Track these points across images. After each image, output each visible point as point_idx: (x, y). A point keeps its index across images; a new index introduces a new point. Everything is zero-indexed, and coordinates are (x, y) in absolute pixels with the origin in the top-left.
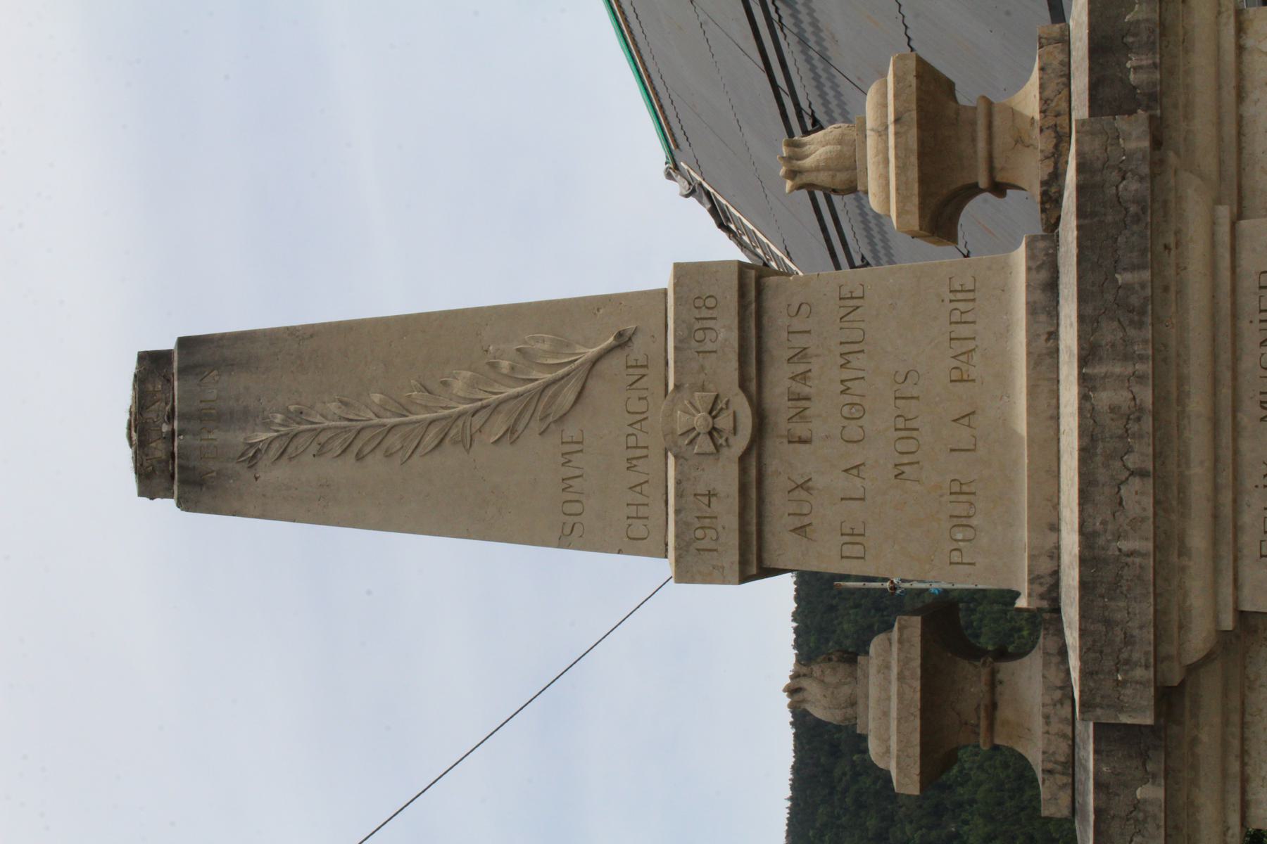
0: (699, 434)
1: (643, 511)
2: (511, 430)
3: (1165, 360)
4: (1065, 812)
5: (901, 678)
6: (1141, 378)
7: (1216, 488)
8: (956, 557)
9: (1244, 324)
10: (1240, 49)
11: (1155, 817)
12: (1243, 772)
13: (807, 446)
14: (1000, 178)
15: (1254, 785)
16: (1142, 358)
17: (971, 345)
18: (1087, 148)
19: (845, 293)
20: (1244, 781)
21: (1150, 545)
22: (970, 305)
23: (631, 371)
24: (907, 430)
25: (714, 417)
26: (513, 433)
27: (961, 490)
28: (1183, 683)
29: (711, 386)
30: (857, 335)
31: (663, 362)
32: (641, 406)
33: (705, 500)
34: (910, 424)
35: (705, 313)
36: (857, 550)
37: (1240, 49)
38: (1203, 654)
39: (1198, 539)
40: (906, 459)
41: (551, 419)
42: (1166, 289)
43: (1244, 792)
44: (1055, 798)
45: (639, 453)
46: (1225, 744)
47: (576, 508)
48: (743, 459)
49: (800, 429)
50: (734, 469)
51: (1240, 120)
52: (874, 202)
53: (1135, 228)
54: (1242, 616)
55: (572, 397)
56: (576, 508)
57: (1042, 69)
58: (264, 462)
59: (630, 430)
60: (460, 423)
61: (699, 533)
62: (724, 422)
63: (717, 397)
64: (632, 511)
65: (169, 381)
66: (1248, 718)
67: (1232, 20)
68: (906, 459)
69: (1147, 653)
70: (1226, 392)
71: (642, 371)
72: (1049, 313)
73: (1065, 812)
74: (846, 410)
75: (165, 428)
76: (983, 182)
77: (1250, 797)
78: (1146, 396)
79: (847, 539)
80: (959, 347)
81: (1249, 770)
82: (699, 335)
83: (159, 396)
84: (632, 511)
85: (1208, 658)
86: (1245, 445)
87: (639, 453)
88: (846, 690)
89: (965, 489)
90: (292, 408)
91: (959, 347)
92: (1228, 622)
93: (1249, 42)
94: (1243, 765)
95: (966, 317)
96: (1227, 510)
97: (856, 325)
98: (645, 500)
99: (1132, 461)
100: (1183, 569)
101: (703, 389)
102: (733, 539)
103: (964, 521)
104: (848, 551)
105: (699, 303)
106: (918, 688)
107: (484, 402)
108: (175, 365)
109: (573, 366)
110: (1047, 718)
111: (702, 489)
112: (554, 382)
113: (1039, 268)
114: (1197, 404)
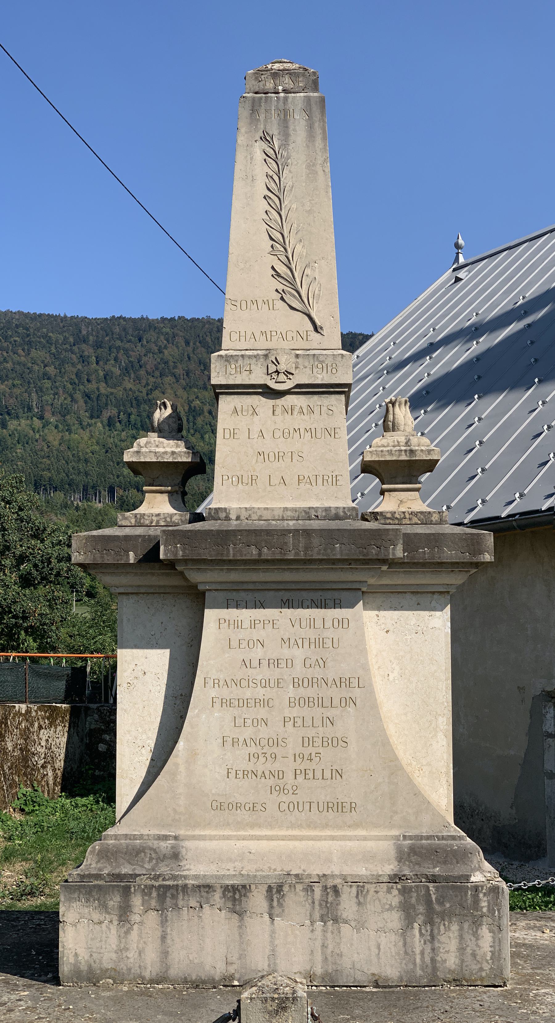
0: (276, 366)
1: (243, 339)
2: (279, 275)
3: (305, 563)
4: (120, 523)
5: (173, 453)
6: (297, 554)
7: (254, 582)
8: (225, 478)
9: (320, 593)
10: (433, 593)
11: (121, 559)
12: (140, 593)
13: (272, 414)
14: (386, 493)
15: (135, 597)
16: (306, 554)
17: (314, 484)
18: (391, 533)
19: (337, 430)
20: (137, 594)
21: (231, 558)
22: (330, 483)
23: (305, 333)
24: (278, 457)
25: (284, 373)
26: (277, 275)
27: (253, 480)
28: (176, 569)
29: (297, 371)
30: (319, 435)
31: (309, 348)
32: (289, 338)
33: (248, 369)
34: (281, 458)
35: (329, 369)
36: (227, 436)
37: (433, 593)
38: (188, 577)
39: (234, 576)
40: (266, 457)
41: (283, 294)
42: (334, 564)
43: (132, 593)
44: (126, 519)
45: (269, 336)
46: (151, 586)
47: (244, 307)
48: (265, 386)
49: (279, 410)
50: (261, 382)
51: (405, 593)
52: (377, 441)
53: (358, 552)
54: (203, 594)
55: (294, 306)
56: (244, 307)
57: (430, 513)
58: (264, 145)
59: (279, 333)
60: (282, 249)
61: (233, 366)
62: (282, 377)
63: (293, 374)
64: (243, 334)
65: (303, 90)
66: (162, 595)
67: (445, 590)
68: (266, 457)
69: (188, 556)
70: (294, 586)
71: (305, 338)
72: (325, 516)
73: (120, 523)
74: (286, 431)
75: (280, 88)
76: (385, 486)
77: (131, 596)
78: (291, 556)
79: (232, 431)
80: (313, 479)
81: (141, 595)
82: (320, 366)
83: (297, 84)
84: (243, 334)
85: (186, 579)
86: (271, 593)
87: (269, 336)
88: (166, 428)
89: (254, 481)
90: (289, 161)
91: (313, 479)
92: (201, 587)
93: (436, 596)
94: (143, 593)
95: (325, 482)
96: (245, 587)
97: (323, 434)
98: (248, 338)
99: (265, 550)
100: (222, 570)
101: (296, 368)
102: (231, 382)
103: (240, 481)
104: (227, 431)
105: (334, 366)
106: (169, 461)
107: (291, 261)
108: (311, 94)
109: (308, 306)
110: (158, 515)
111: (253, 367)
112: (300, 296)
113: (344, 512)
114: (288, 576)
